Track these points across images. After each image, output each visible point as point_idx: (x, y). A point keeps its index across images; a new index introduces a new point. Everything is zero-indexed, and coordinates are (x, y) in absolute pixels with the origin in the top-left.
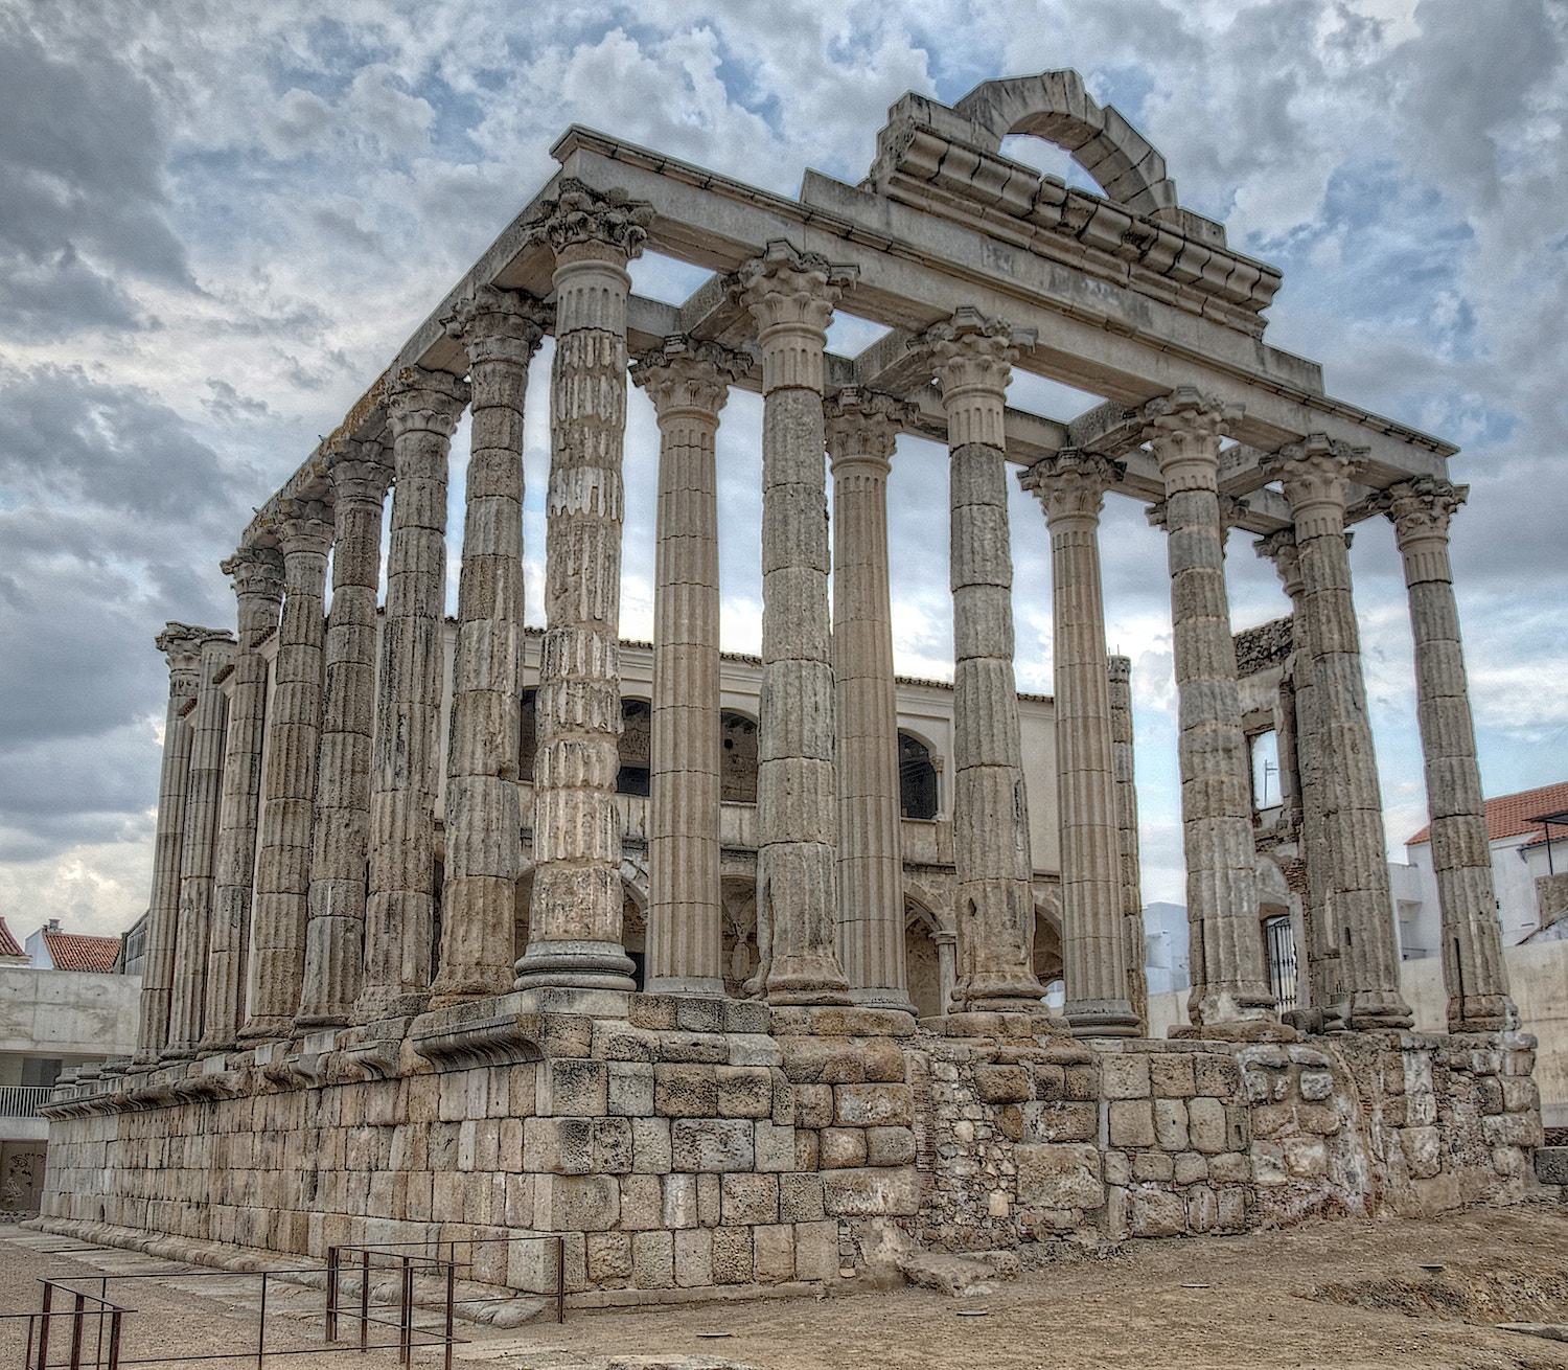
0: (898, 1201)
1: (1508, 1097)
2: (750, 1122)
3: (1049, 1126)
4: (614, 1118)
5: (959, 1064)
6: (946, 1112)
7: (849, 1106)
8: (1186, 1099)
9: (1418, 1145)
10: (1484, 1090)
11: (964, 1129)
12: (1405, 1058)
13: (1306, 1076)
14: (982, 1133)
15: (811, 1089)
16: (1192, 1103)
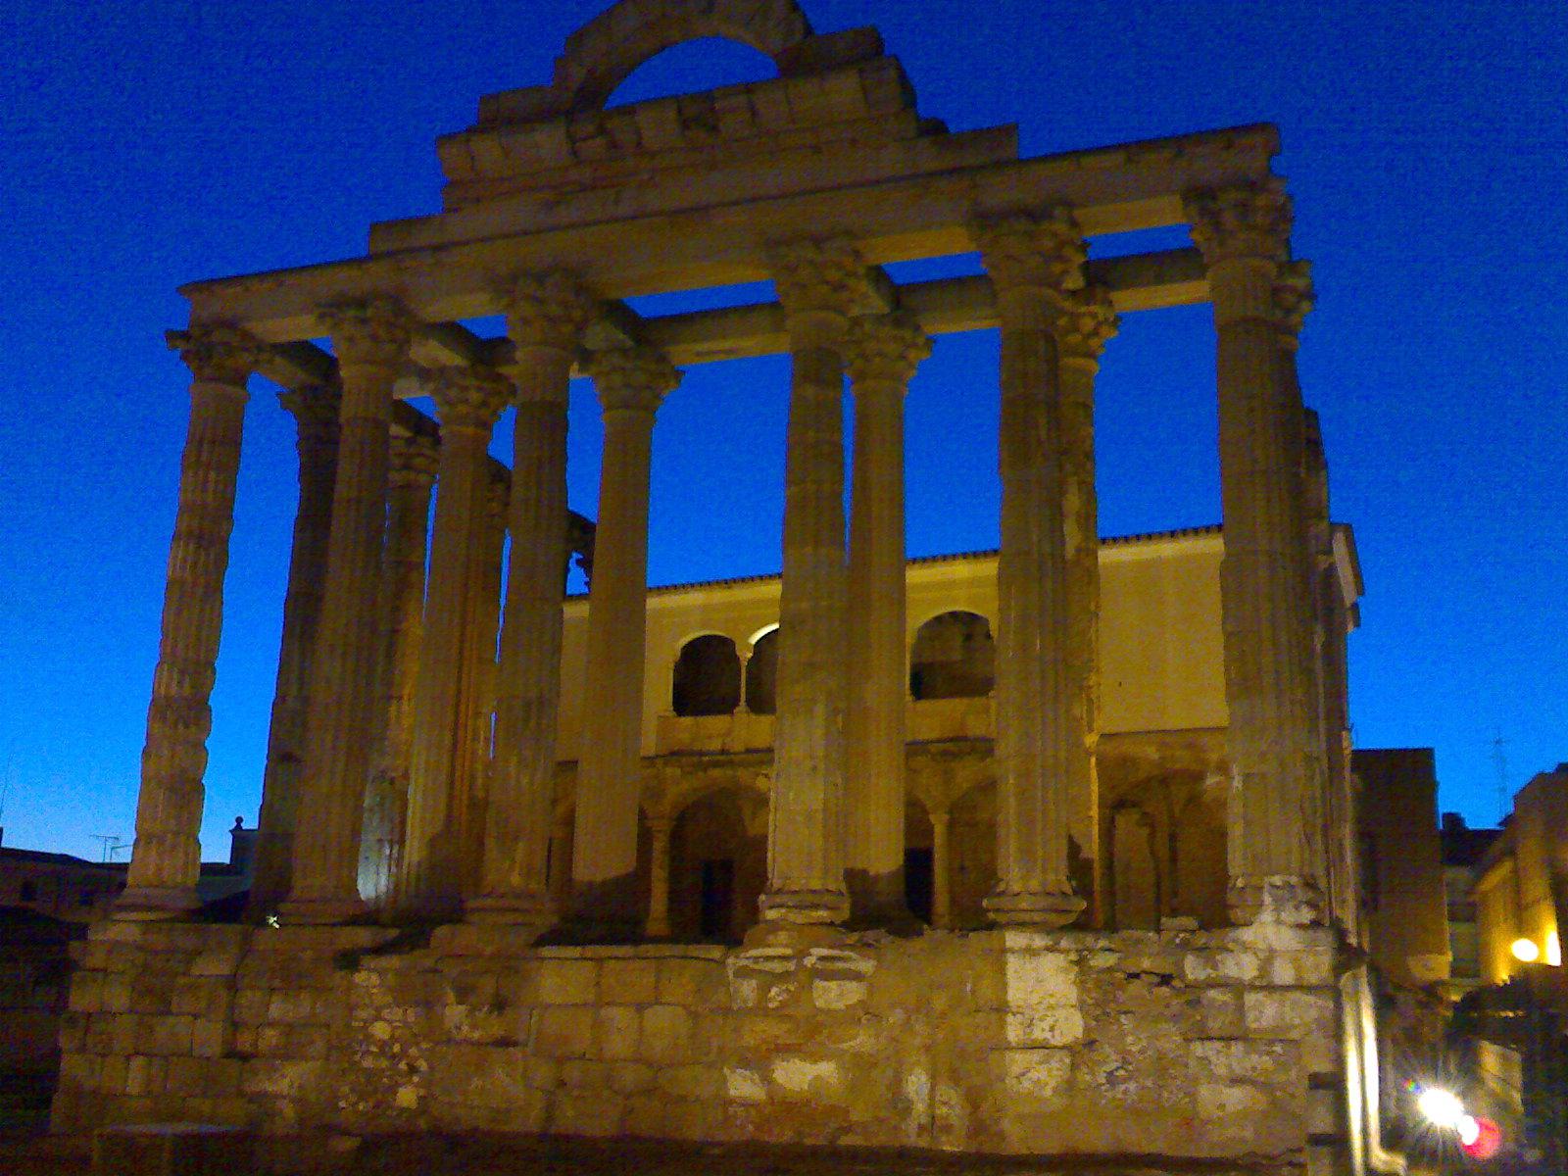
0: (301, 1087)
1: (1251, 1016)
2: (191, 1018)
3: (474, 1027)
4: (107, 1014)
5: (381, 973)
6: (363, 1014)
7: (277, 1009)
8: (640, 1008)
9: (1016, 1070)
10: (1195, 1003)
11: (381, 1030)
12: (1013, 963)
13: (819, 984)
14: (398, 1033)
15: (249, 993)
16: (648, 1013)
